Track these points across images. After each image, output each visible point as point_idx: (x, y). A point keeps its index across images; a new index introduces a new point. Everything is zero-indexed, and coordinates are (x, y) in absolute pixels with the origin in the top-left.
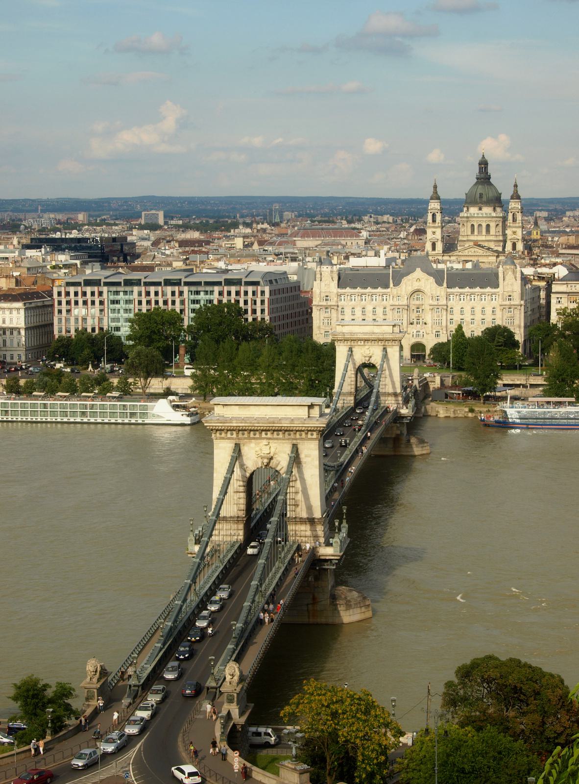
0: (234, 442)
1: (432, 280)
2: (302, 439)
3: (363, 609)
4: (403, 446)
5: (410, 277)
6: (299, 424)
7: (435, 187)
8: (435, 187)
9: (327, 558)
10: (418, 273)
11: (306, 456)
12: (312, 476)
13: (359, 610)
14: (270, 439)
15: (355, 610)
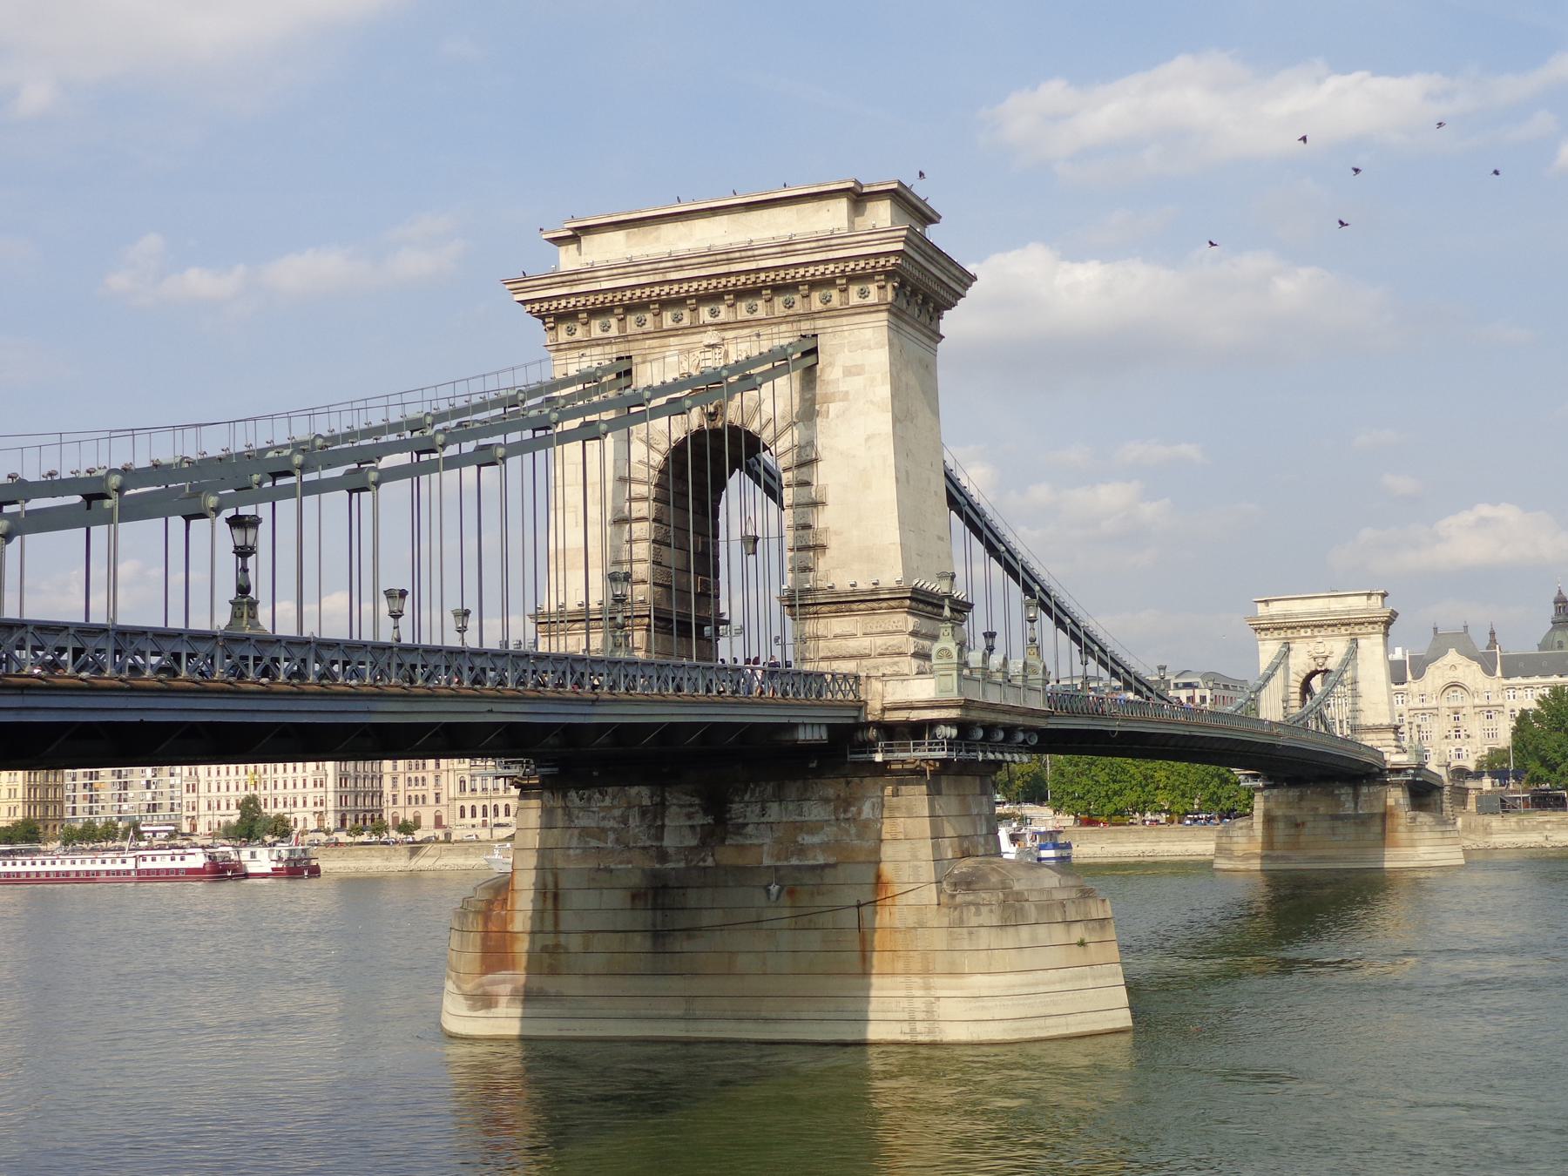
0: (614, 351)
1: (1476, 666)
2: (829, 313)
3: (1078, 932)
4: (1401, 828)
5: (1438, 663)
6: (813, 251)
7: (1492, 634)
8: (1492, 634)
9: (916, 716)
10: (1452, 656)
11: (849, 372)
12: (868, 439)
13: (1059, 934)
14: (723, 326)
15: (1042, 931)
